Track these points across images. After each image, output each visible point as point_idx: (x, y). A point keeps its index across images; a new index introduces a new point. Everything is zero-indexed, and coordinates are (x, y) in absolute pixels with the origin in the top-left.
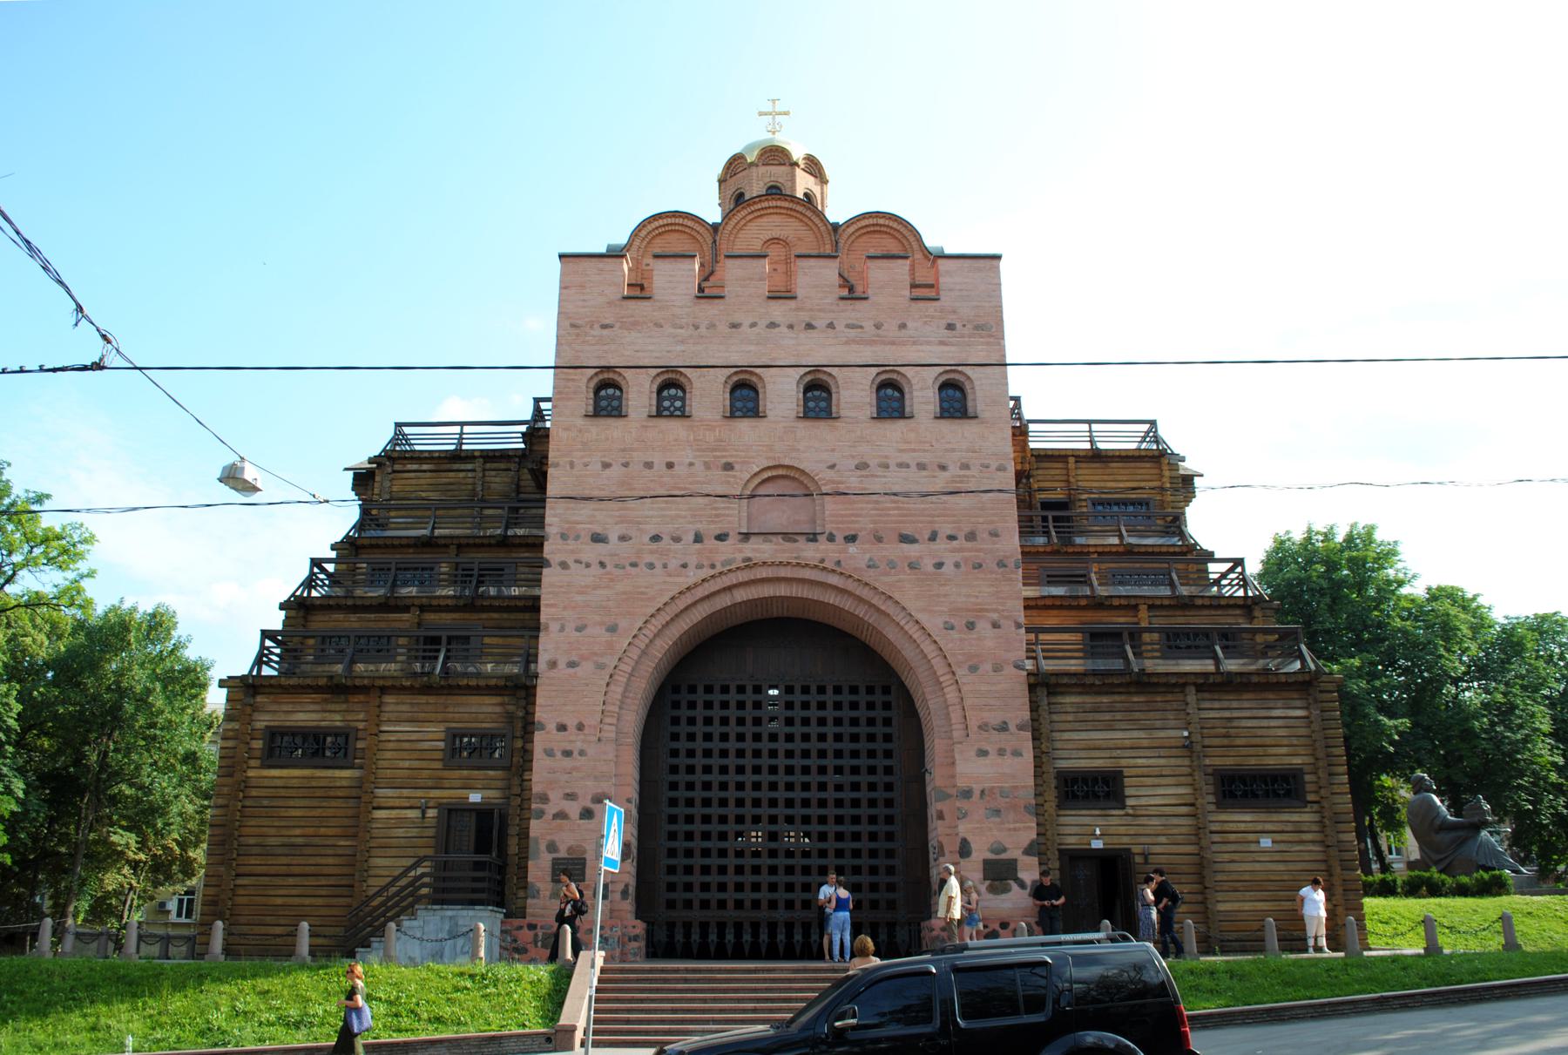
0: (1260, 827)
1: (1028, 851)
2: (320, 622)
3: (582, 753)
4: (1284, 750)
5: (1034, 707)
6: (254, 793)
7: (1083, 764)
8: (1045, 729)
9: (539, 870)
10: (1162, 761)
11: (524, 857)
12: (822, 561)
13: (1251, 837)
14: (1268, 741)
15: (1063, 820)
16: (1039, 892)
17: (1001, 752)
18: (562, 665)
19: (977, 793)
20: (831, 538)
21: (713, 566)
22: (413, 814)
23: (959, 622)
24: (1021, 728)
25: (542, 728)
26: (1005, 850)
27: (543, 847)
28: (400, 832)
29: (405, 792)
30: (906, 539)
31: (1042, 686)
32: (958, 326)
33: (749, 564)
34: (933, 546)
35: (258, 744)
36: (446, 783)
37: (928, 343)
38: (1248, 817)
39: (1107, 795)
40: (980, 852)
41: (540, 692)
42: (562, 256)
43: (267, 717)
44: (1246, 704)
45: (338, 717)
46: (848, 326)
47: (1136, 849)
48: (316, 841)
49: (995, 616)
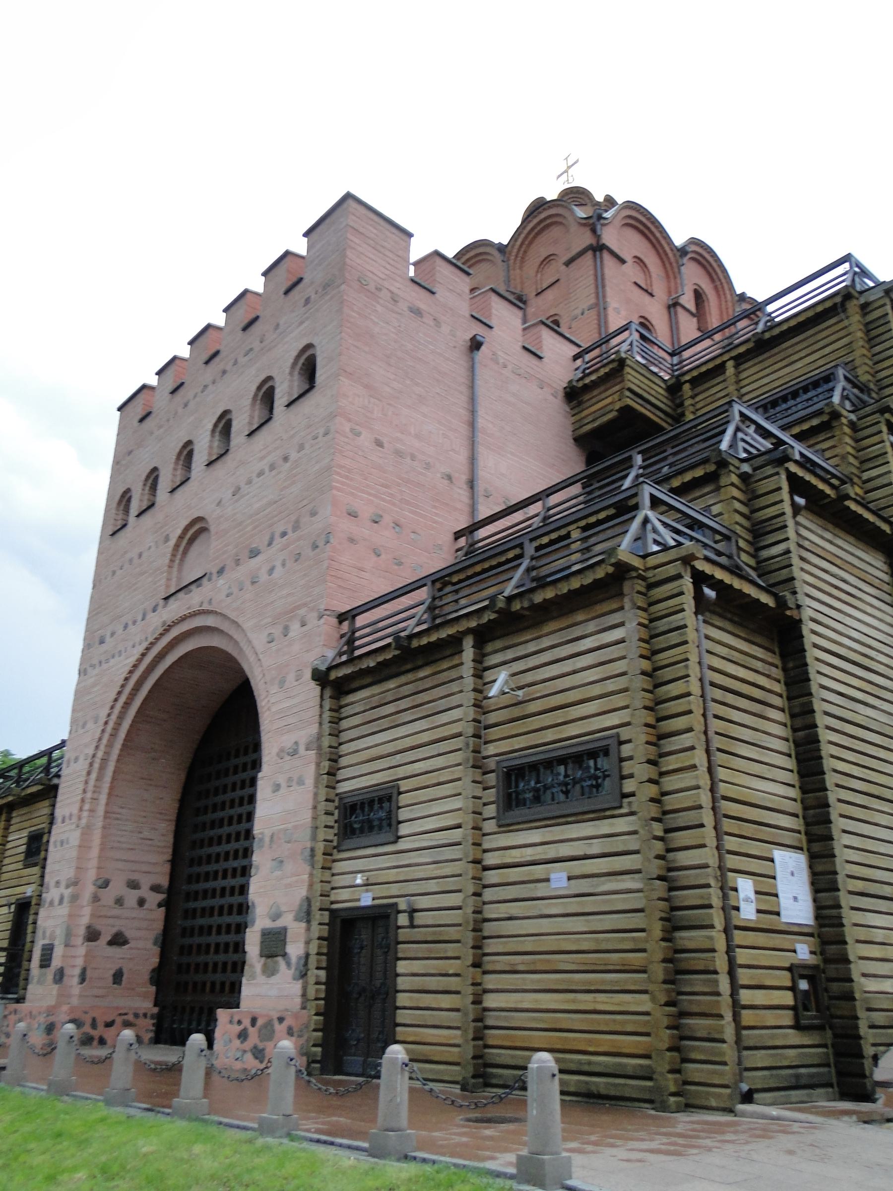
0: (552, 852)
1: (297, 919)
12: (201, 604)
13: (538, 871)
15: (339, 867)
23: (277, 631)
38: (535, 836)
44: (546, 642)
47: (403, 905)
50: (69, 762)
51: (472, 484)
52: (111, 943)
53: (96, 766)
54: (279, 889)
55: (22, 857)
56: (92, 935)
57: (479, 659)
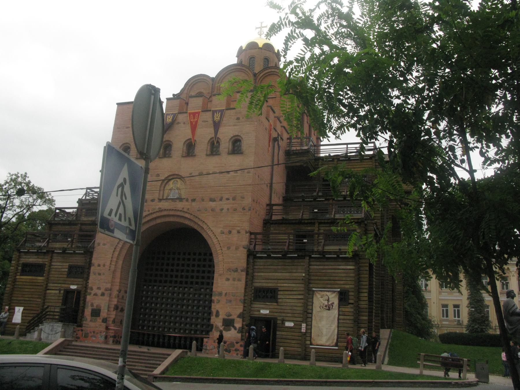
1: (239, 316)
2: (55, 228)
3: (104, 274)
4: (342, 282)
5: (248, 263)
6: (17, 283)
7: (264, 285)
8: (250, 271)
9: (88, 312)
10: (294, 285)
11: (84, 307)
12: (183, 209)
14: (337, 278)
16: (241, 331)
17: (234, 280)
18: (101, 245)
19: (224, 294)
20: (187, 200)
21: (149, 211)
22: (57, 292)
24: (242, 271)
25: (94, 265)
26: (231, 315)
27: (89, 305)
28: (53, 298)
29: (56, 285)
31: (251, 255)
32: (241, 118)
33: (161, 210)
34: (221, 202)
35: (20, 268)
36: (67, 282)
37: (229, 126)
39: (271, 297)
40: (222, 316)
41: (94, 253)
42: (117, 104)
43: (24, 260)
45: (41, 260)
46: (203, 121)
47: (279, 318)
48: (31, 299)
49: (239, 228)
50: (99, 244)
52: (120, 311)
53: (118, 249)
55: (66, 273)
56: (116, 308)
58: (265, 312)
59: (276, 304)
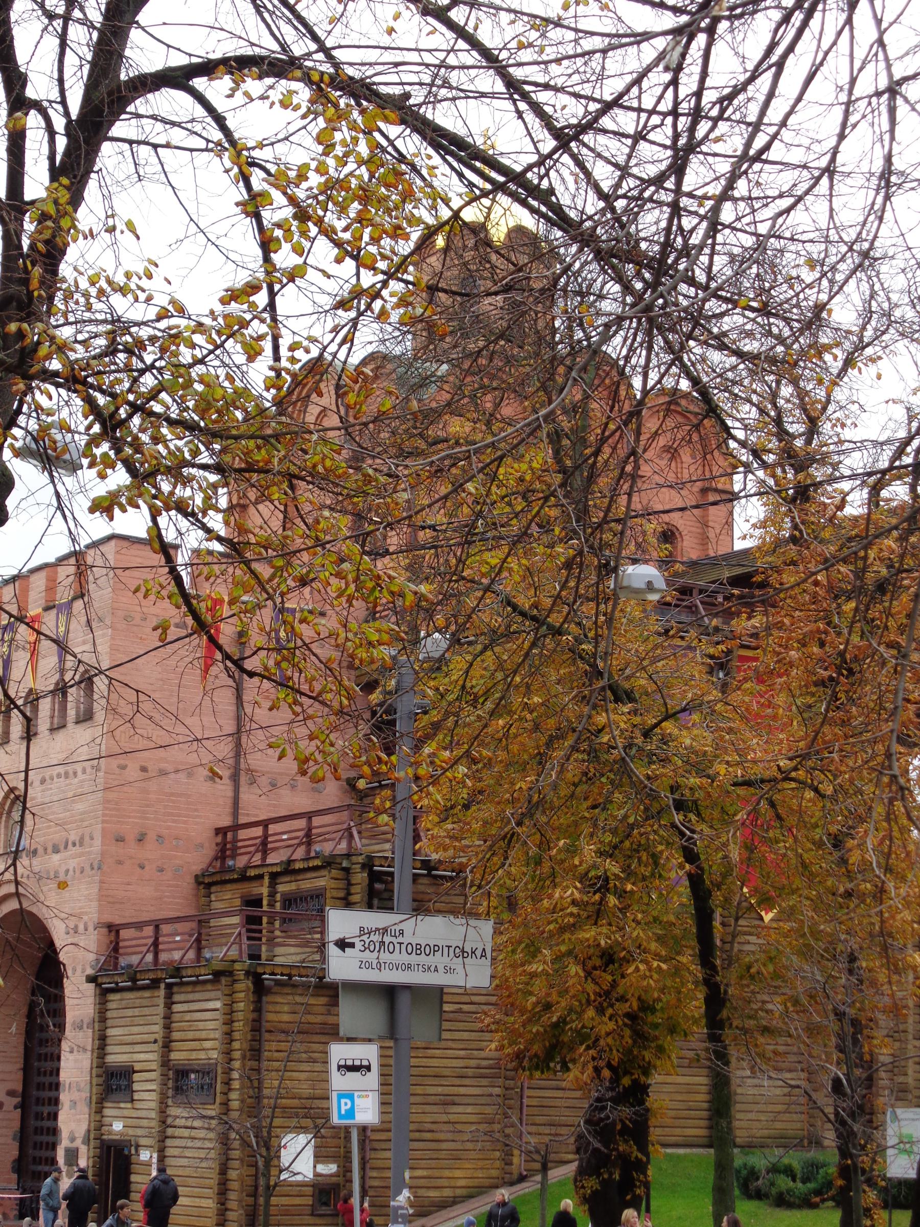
14: (203, 1035)
30: (56, 850)
51: (235, 778)
54: (73, 1122)
57: (169, 996)
58: (118, 1126)
59: (129, 1105)
